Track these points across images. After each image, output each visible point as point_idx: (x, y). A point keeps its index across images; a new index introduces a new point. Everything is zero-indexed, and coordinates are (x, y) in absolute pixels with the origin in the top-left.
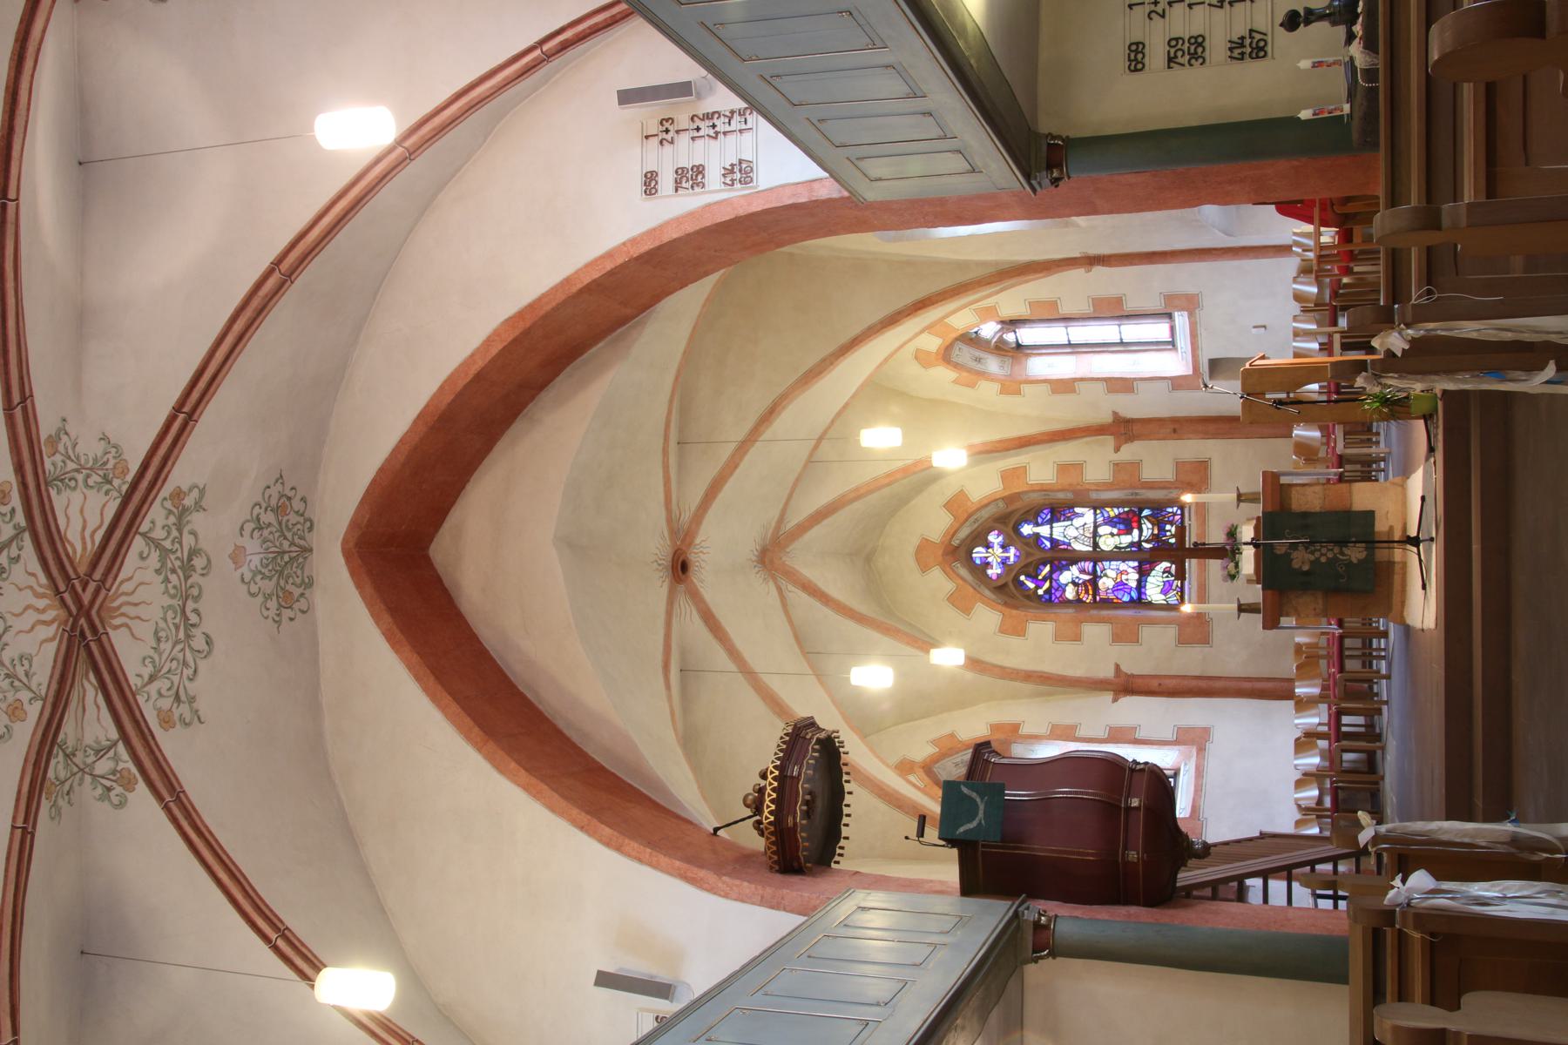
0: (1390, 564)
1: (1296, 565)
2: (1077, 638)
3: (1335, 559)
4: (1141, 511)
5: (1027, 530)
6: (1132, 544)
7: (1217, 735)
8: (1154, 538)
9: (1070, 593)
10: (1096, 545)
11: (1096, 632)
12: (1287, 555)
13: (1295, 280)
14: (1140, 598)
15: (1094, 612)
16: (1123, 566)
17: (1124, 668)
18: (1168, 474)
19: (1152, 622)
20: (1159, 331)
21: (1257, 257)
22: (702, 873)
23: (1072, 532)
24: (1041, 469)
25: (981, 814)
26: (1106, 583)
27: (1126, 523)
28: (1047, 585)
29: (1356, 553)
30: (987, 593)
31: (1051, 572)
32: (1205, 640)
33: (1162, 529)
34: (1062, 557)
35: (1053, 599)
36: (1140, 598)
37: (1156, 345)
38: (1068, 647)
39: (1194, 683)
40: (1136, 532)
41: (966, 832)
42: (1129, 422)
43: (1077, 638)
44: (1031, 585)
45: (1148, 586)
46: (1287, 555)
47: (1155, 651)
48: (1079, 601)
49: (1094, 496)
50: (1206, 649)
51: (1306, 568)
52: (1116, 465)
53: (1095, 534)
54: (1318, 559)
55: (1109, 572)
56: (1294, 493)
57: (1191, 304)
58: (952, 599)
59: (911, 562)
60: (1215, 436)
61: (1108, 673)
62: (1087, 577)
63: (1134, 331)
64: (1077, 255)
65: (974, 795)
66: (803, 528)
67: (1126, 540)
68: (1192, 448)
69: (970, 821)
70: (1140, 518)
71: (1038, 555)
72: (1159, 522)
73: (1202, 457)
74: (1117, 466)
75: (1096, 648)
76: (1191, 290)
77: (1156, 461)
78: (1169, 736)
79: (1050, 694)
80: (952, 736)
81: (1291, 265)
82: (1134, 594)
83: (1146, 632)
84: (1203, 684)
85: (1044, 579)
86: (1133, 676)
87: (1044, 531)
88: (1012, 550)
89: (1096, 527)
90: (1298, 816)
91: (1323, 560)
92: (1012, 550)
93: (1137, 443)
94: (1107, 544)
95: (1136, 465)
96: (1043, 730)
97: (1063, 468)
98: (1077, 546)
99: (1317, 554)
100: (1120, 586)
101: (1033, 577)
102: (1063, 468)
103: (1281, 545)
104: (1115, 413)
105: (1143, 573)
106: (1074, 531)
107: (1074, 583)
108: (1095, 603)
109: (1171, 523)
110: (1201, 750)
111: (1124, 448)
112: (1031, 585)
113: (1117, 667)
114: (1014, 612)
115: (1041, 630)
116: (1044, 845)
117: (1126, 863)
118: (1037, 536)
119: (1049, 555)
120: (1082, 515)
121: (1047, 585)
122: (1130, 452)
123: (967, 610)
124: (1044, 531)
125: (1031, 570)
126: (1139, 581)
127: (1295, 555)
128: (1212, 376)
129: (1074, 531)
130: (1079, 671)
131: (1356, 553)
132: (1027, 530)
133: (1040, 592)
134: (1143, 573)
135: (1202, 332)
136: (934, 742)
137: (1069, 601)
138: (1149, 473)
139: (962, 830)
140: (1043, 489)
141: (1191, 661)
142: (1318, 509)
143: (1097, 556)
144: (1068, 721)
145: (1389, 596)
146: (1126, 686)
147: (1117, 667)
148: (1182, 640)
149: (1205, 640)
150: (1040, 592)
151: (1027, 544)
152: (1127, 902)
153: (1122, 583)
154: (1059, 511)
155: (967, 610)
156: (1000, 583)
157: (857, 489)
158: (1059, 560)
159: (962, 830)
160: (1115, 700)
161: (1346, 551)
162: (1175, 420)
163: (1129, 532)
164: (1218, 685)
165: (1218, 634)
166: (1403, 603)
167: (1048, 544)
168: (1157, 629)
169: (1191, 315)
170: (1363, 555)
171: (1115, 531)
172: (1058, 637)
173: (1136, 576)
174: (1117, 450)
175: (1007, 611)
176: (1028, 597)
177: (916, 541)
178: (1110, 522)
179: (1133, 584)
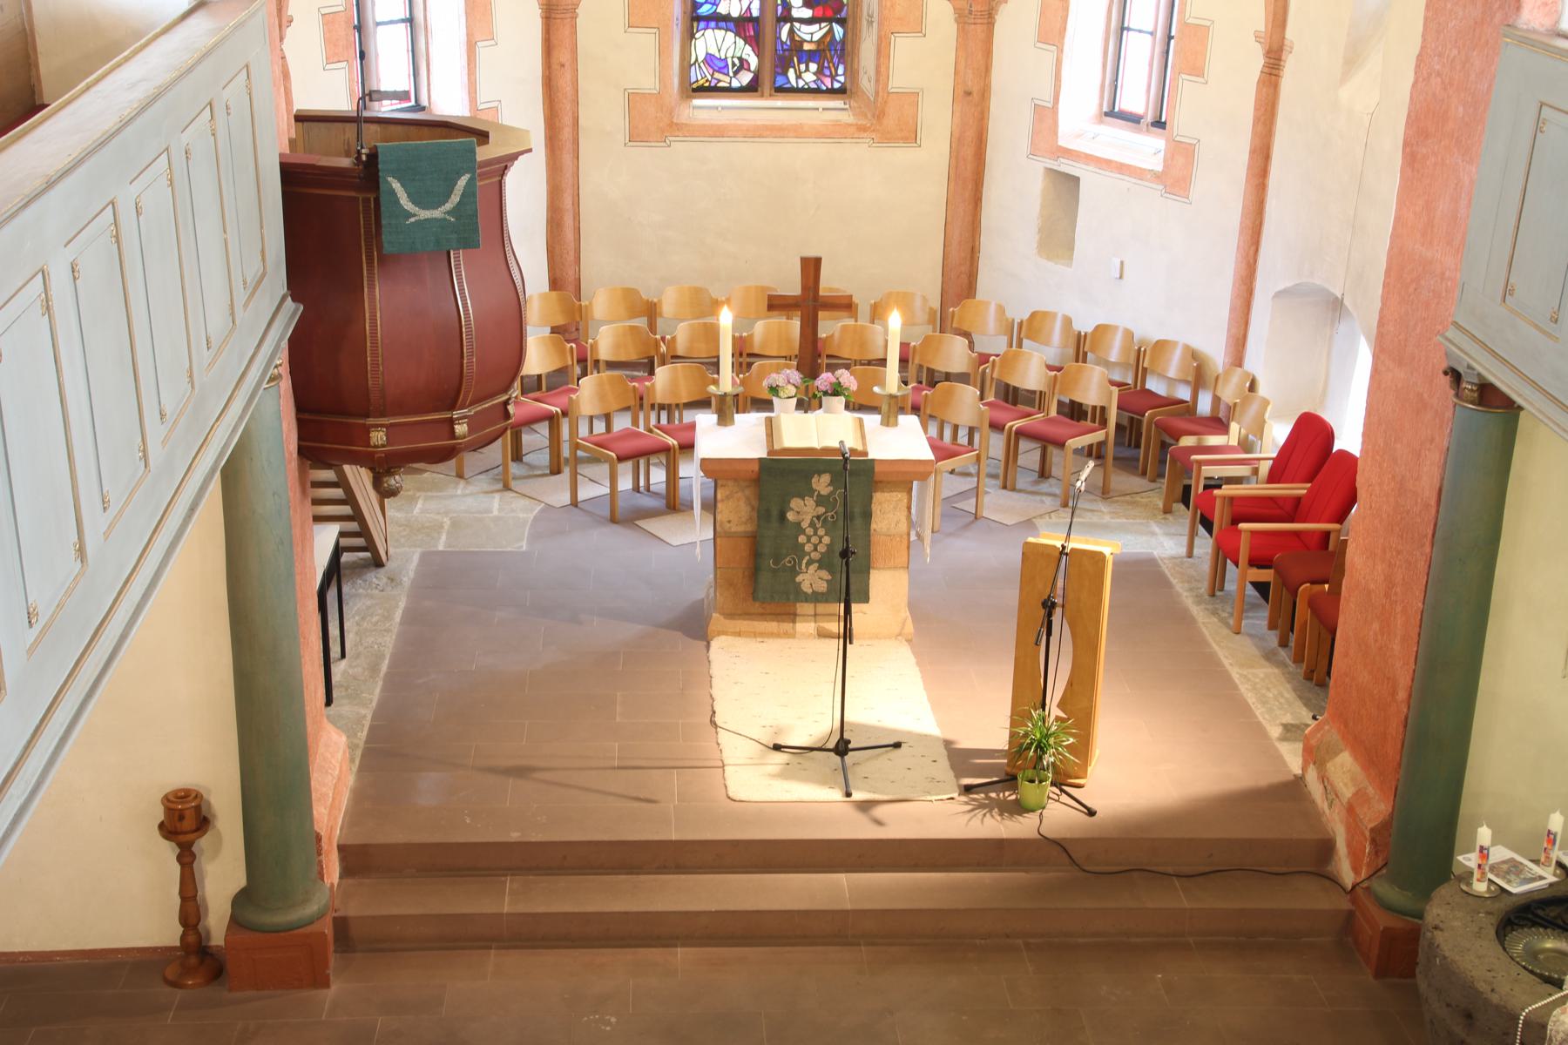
0: (793, 617)
1: (795, 503)
4: (842, 22)
8: (796, 44)
12: (810, 492)
13: (1187, 347)
14: (699, 19)
18: (899, 80)
19: (663, 52)
20: (1135, 98)
21: (1232, 309)
25: (425, 214)
29: (812, 579)
33: (812, 56)
36: (699, 19)
37: (1113, 86)
39: (567, 120)
41: (393, 192)
46: (810, 492)
50: (621, 136)
51: (790, 516)
54: (803, 532)
56: (899, 497)
57: (1176, 177)
63: (1139, 52)
64: (1289, 34)
65: (455, 198)
68: (938, 122)
70: (830, 20)
72: (825, 53)
73: (923, 135)
76: (1198, 188)
81: (1216, 351)
82: (705, 10)
83: (646, 40)
84: (566, 134)
86: (574, 18)
95: (918, 29)
99: (810, 531)
103: (822, 484)
109: (819, 73)
116: (385, 304)
117: (367, 430)
126: (726, 18)
127: (810, 502)
128: (1050, 171)
131: (812, 579)
135: (1127, 182)
138: (903, 49)
139: (396, 185)
141: (601, 113)
142: (873, 526)
145: (747, 615)
148: (634, 99)
152: (301, 423)
159: (396, 185)
162: (985, 93)
164: (567, 158)
165: (644, 155)
166: (739, 634)
169: (1158, 177)
170: (806, 588)
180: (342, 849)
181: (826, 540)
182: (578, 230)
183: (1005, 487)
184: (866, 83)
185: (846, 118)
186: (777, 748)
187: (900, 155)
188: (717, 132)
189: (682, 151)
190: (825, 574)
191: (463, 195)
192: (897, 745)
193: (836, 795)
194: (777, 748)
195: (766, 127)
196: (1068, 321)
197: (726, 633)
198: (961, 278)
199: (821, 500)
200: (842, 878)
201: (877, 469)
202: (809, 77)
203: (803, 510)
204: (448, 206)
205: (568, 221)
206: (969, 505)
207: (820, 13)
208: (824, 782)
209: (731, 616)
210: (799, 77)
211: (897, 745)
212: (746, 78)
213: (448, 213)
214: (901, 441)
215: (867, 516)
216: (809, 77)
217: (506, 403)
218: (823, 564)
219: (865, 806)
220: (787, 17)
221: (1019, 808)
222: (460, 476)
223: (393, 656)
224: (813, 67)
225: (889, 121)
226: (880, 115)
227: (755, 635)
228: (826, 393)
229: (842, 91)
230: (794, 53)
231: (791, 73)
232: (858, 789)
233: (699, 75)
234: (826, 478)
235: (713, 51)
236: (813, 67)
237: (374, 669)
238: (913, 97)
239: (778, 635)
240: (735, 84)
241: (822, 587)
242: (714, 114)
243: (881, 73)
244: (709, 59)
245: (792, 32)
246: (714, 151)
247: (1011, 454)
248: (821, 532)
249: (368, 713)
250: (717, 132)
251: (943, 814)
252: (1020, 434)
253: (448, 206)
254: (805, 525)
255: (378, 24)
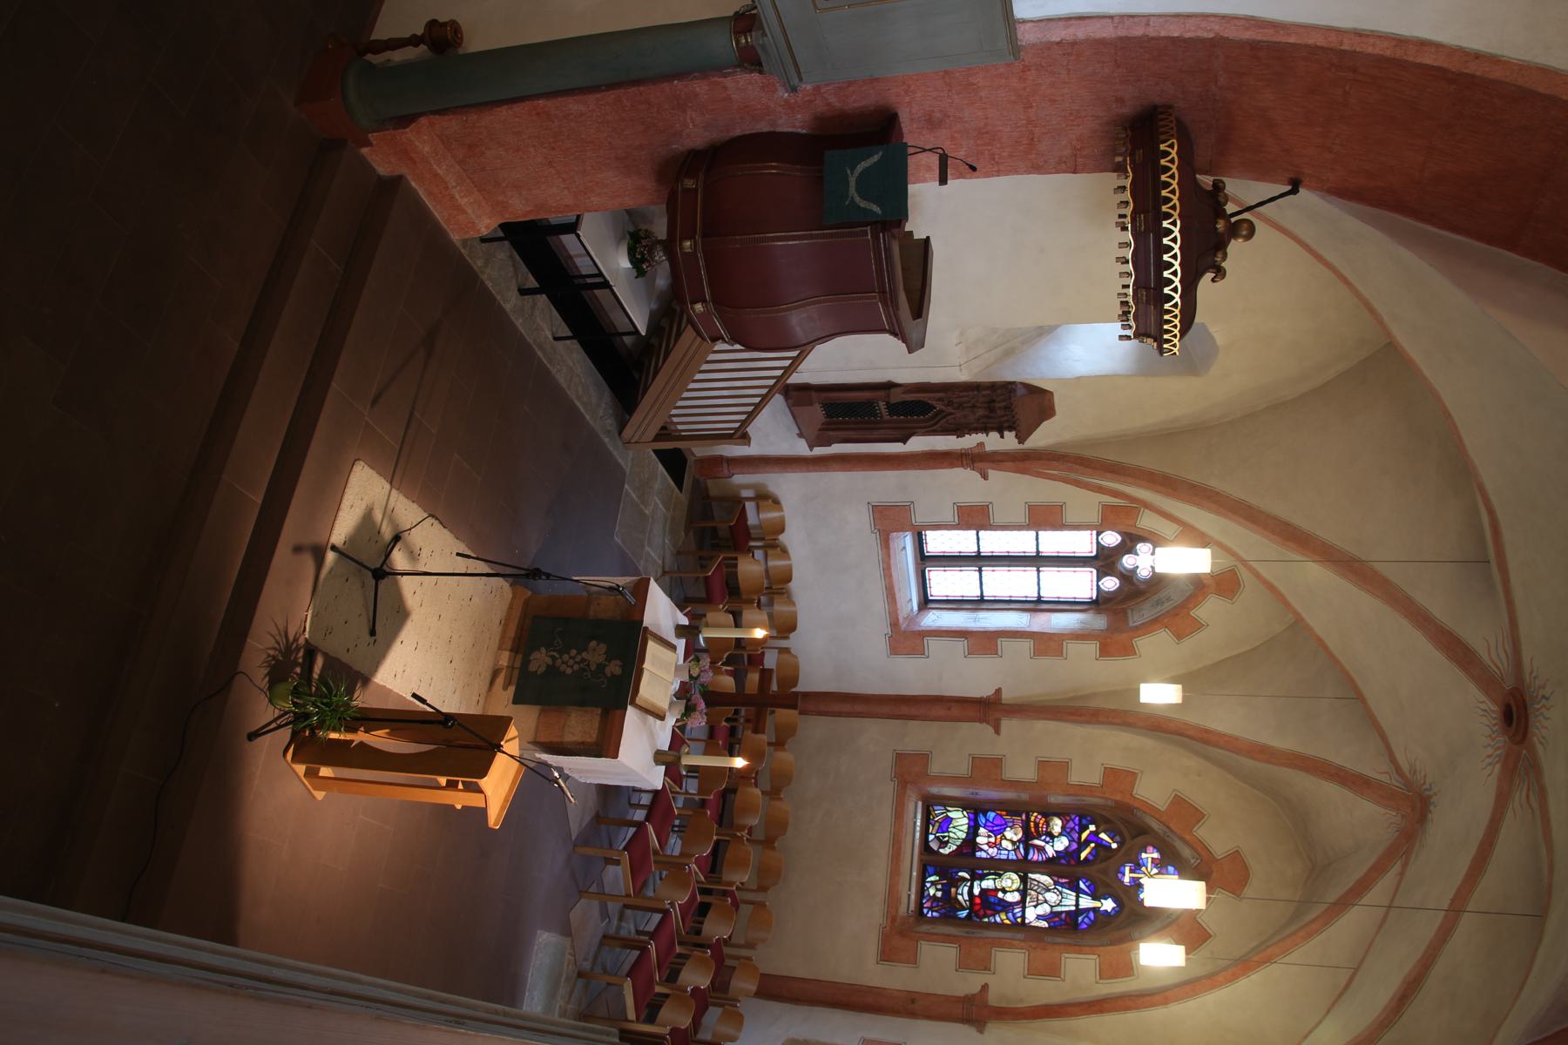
0: (515, 650)
1: (603, 647)
2: (1042, 765)
3: (561, 653)
5: (1108, 905)
6: (982, 878)
7: (882, 645)
9: (1057, 825)
10: (1024, 880)
11: (1022, 769)
12: (609, 660)
14: (976, 815)
15: (1024, 796)
16: (993, 852)
17: (990, 730)
22: (1247, 35)
23: (1049, 896)
24: (1080, 971)
26: (1013, 834)
27: (989, 902)
28: (1084, 836)
29: (540, 659)
30: (1155, 825)
31: (1079, 851)
32: (900, 757)
34: (1065, 869)
35: (1077, 817)
36: (976, 815)
38: (1056, 755)
40: (976, 891)
41: (869, 156)
42: (966, 1020)
43: (1042, 765)
44: (1103, 836)
45: (965, 828)
46: (609, 660)
47: (953, 750)
48: (1048, 815)
49: (1020, 936)
51: (593, 644)
52: (987, 968)
53: (1024, 893)
54: (579, 653)
55: (1010, 847)
58: (1197, 816)
59: (1255, 866)
60: (871, 990)
61: (1006, 724)
62: (1036, 842)
65: (863, 204)
66: (1378, 869)
67: (988, 884)
68: (896, 978)
69: (866, 169)
70: (971, 908)
71: (1092, 870)
72: (948, 903)
74: (985, 966)
75: (1022, 752)
77: (937, 966)
78: (933, 644)
79: (1072, 699)
80: (1179, 636)
82: (982, 820)
83: (963, 769)
84: (904, 710)
85: (1087, 842)
86: (981, 721)
87: (1086, 902)
88: (1126, 880)
89: (1023, 902)
90: (782, 538)
91: (574, 652)
92: (1126, 880)
93: (960, 993)
94: (1011, 881)
95: (963, 965)
96: (1072, 648)
97: (1053, 971)
98: (1046, 879)
99: (578, 659)
100: (998, 830)
101: (1100, 843)
102: (1053, 971)
103: (614, 668)
104: (981, 1031)
105: (970, 843)
106: (1050, 900)
107: (1052, 837)
108: (1027, 810)
110: (895, 624)
111: (976, 989)
112: (1103, 836)
113: (997, 732)
114: (1118, 797)
115: (1086, 773)
118: (1095, 898)
119: (1080, 869)
120: (1039, 917)
121: (1084, 836)
122: (969, 984)
123: (1178, 802)
124: (1086, 902)
125: (1102, 853)
129: (1050, 900)
130: (1040, 725)
131: (540, 659)
132: (1108, 905)
133: (1092, 828)
134: (970, 843)
136: (1197, 626)
137: (1058, 815)
139: (876, 158)
140: (1079, 948)
141: (916, 735)
143: (1023, 867)
144: (1045, 662)
146: (988, 709)
147: (997, 732)
148: (924, 758)
149: (900, 757)
150: (1092, 828)
151: (1108, 885)
153: (996, 833)
154: (1064, 924)
155: (1178, 802)
156: (1140, 840)
157: (1310, 935)
158: (1069, 864)
159: (876, 158)
160: (998, 691)
161: (550, 661)
162: (912, 1015)
163: (983, 891)
165: (886, 763)
166: (511, 607)
167: (1082, 885)
168: (950, 772)
171: (1000, 895)
172: (1065, 766)
173: (979, 840)
174: (985, 987)
175: (1127, 800)
176: (1107, 821)
177: (1248, 891)
178: (1007, 907)
179: (982, 830)
180: (400, 178)
181: (569, 671)
182: (839, 714)
183: (604, 936)
184: (925, 928)
185: (902, 910)
186: (397, 538)
187: (872, 947)
188: (899, 814)
189: (889, 788)
190: (543, 669)
191: (865, 209)
192: (373, 633)
193: (339, 535)
194: (397, 538)
195: (899, 849)
196: (733, 1039)
197: (514, 598)
198: (777, 990)
199: (601, 667)
200: (258, 499)
201: (618, 712)
202: (932, 892)
203: (596, 653)
204: (857, 199)
205: (846, 707)
206: (593, 889)
207: (978, 901)
208: (352, 540)
209: (526, 603)
210: (933, 883)
211: (373, 633)
212: (934, 846)
213: (853, 201)
214: (638, 757)
215: (582, 704)
216: (932, 892)
217: (704, 301)
218: (552, 670)
219: (319, 553)
220: (975, 877)
221: (277, 673)
222: (679, 553)
223: (549, 372)
224: (939, 894)
225: (900, 937)
226: (903, 934)
227: (508, 618)
228: (689, 700)
229: (921, 914)
230: (951, 882)
231: (933, 878)
232: (337, 562)
233: (938, 810)
234: (618, 671)
235: (955, 823)
236: (939, 894)
237: (541, 348)
238: (913, 960)
239: (504, 632)
240: (931, 837)
241: (532, 668)
242: (910, 830)
243: (930, 937)
244: (950, 820)
245: (964, 879)
246: (886, 811)
247: (628, 944)
248: (576, 667)
249: (508, 307)
250: (899, 814)
251: (293, 607)
252: (644, 950)
253: (857, 199)
254: (584, 654)
255: (980, 571)
